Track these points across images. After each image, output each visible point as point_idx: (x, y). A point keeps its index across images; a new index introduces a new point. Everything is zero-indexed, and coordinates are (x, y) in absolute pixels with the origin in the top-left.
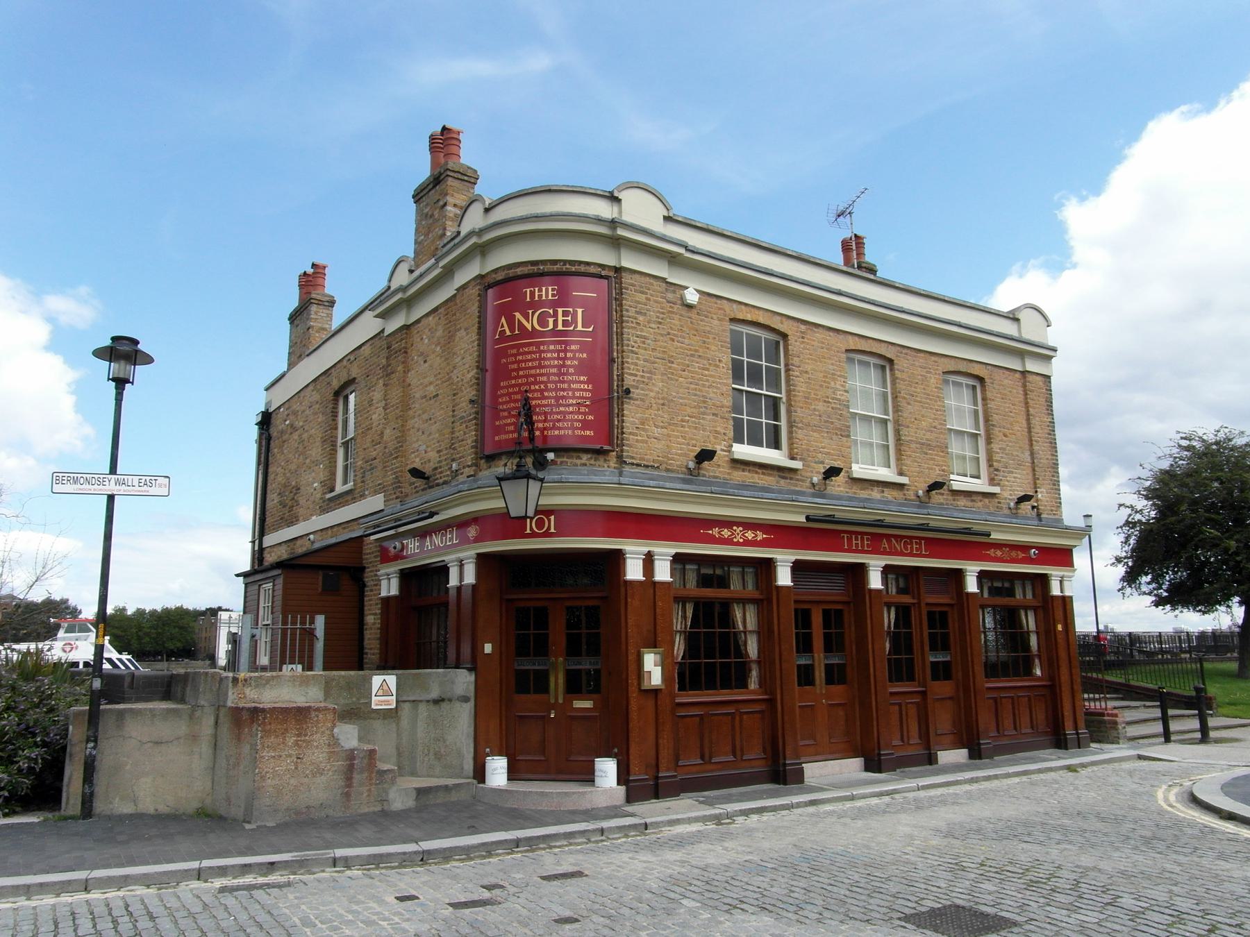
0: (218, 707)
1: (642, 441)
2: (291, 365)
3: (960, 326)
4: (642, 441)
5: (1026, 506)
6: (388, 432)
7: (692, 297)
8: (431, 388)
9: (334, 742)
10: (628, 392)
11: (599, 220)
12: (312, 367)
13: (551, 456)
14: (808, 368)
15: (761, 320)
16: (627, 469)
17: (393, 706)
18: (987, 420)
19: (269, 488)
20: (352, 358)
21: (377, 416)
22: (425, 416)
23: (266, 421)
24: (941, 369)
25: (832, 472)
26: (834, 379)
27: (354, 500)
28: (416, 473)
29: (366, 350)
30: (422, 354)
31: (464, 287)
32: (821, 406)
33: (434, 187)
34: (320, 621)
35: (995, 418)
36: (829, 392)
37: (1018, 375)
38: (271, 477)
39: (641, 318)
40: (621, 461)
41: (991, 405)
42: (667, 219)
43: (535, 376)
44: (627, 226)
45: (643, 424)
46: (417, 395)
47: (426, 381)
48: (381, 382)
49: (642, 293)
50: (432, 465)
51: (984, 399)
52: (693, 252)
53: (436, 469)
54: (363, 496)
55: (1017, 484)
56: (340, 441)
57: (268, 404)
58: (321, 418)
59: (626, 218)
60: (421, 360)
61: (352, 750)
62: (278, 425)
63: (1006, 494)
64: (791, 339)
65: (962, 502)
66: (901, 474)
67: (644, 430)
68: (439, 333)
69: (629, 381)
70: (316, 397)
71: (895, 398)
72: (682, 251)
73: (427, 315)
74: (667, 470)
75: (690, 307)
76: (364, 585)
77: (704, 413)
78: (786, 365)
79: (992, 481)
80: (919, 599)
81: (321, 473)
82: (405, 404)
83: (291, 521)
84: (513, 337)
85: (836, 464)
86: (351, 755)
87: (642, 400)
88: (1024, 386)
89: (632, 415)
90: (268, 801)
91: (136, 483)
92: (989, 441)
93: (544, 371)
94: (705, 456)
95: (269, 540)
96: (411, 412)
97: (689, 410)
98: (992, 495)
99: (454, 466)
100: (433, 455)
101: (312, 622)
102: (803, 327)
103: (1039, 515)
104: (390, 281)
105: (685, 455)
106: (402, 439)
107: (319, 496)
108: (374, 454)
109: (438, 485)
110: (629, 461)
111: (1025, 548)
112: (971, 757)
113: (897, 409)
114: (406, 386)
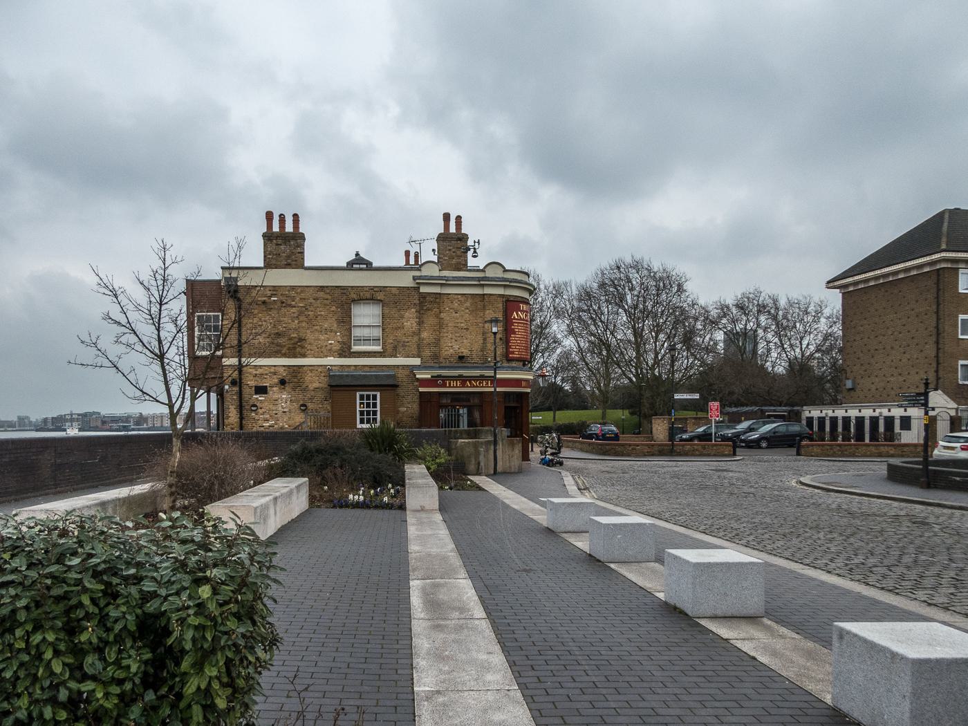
6: (425, 335)
8: (462, 325)
22: (458, 335)
27: (384, 357)
28: (461, 358)
29: (394, 291)
31: (491, 295)
33: (457, 241)
46: (450, 325)
47: (457, 321)
48: (413, 310)
58: (334, 308)
68: (468, 304)
82: (441, 325)
84: (517, 319)
108: (407, 340)
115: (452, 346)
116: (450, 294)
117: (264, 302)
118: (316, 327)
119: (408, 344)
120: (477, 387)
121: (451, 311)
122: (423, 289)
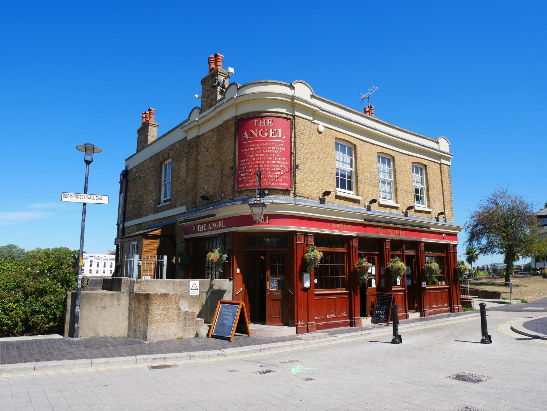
0: (131, 292)
1: (303, 187)
2: (138, 151)
3: (419, 144)
4: (303, 187)
5: (441, 217)
6: (189, 180)
7: (321, 128)
8: (210, 162)
9: (179, 309)
10: (298, 166)
11: (286, 96)
12: (147, 153)
13: (267, 192)
14: (364, 159)
15: (346, 139)
16: (297, 198)
17: (198, 294)
18: (427, 182)
19: (127, 202)
20: (170, 149)
21: (183, 173)
22: (207, 174)
23: (125, 174)
24: (411, 161)
25: (374, 201)
26: (373, 164)
28: (204, 198)
30: (206, 148)
31: (227, 121)
32: (368, 175)
33: (211, 78)
34: (165, 257)
35: (430, 182)
36: (371, 169)
37: (439, 165)
38: (128, 198)
39: (302, 136)
40: (295, 196)
41: (429, 176)
42: (312, 96)
43: (259, 157)
44: (298, 99)
45: (303, 179)
46: (203, 165)
47: (208, 159)
49: (303, 126)
50: (211, 194)
51: (426, 174)
52: (322, 110)
53: (212, 196)
54: (175, 207)
55: (437, 208)
56: (163, 183)
57: (127, 167)
58: (154, 173)
59: (297, 94)
60: (205, 150)
61: (185, 312)
62: (131, 177)
63: (434, 212)
64: (358, 148)
65: (419, 214)
66: (397, 203)
67: (304, 182)
68: (214, 139)
69: (298, 162)
70: (151, 164)
71: (395, 172)
72: (319, 109)
73: (208, 132)
74: (312, 199)
75: (320, 133)
76: (176, 243)
77: (326, 176)
78: (355, 157)
79: (429, 206)
80: (403, 252)
81: (154, 195)
83: (140, 216)
85: (376, 199)
86: (186, 313)
87: (303, 170)
88: (441, 169)
89: (299, 175)
90: (153, 332)
91: (95, 198)
92: (428, 190)
93: (264, 155)
94: (327, 193)
95: (127, 224)
96: (200, 172)
97: (320, 175)
98: (429, 212)
99: (223, 195)
100: (211, 190)
101: (162, 258)
102: (362, 142)
103: (445, 220)
104: (189, 116)
105: (318, 193)
106: (196, 183)
107: (153, 206)
109: (213, 202)
110: (298, 195)
111: (440, 233)
112: (421, 316)
113: (395, 177)
114: (197, 161)
115: (207, 186)
116: (204, 134)
117: (134, 179)
118: (147, 191)
119: (181, 193)
120: (215, 229)
121: (205, 150)
122: (191, 135)
